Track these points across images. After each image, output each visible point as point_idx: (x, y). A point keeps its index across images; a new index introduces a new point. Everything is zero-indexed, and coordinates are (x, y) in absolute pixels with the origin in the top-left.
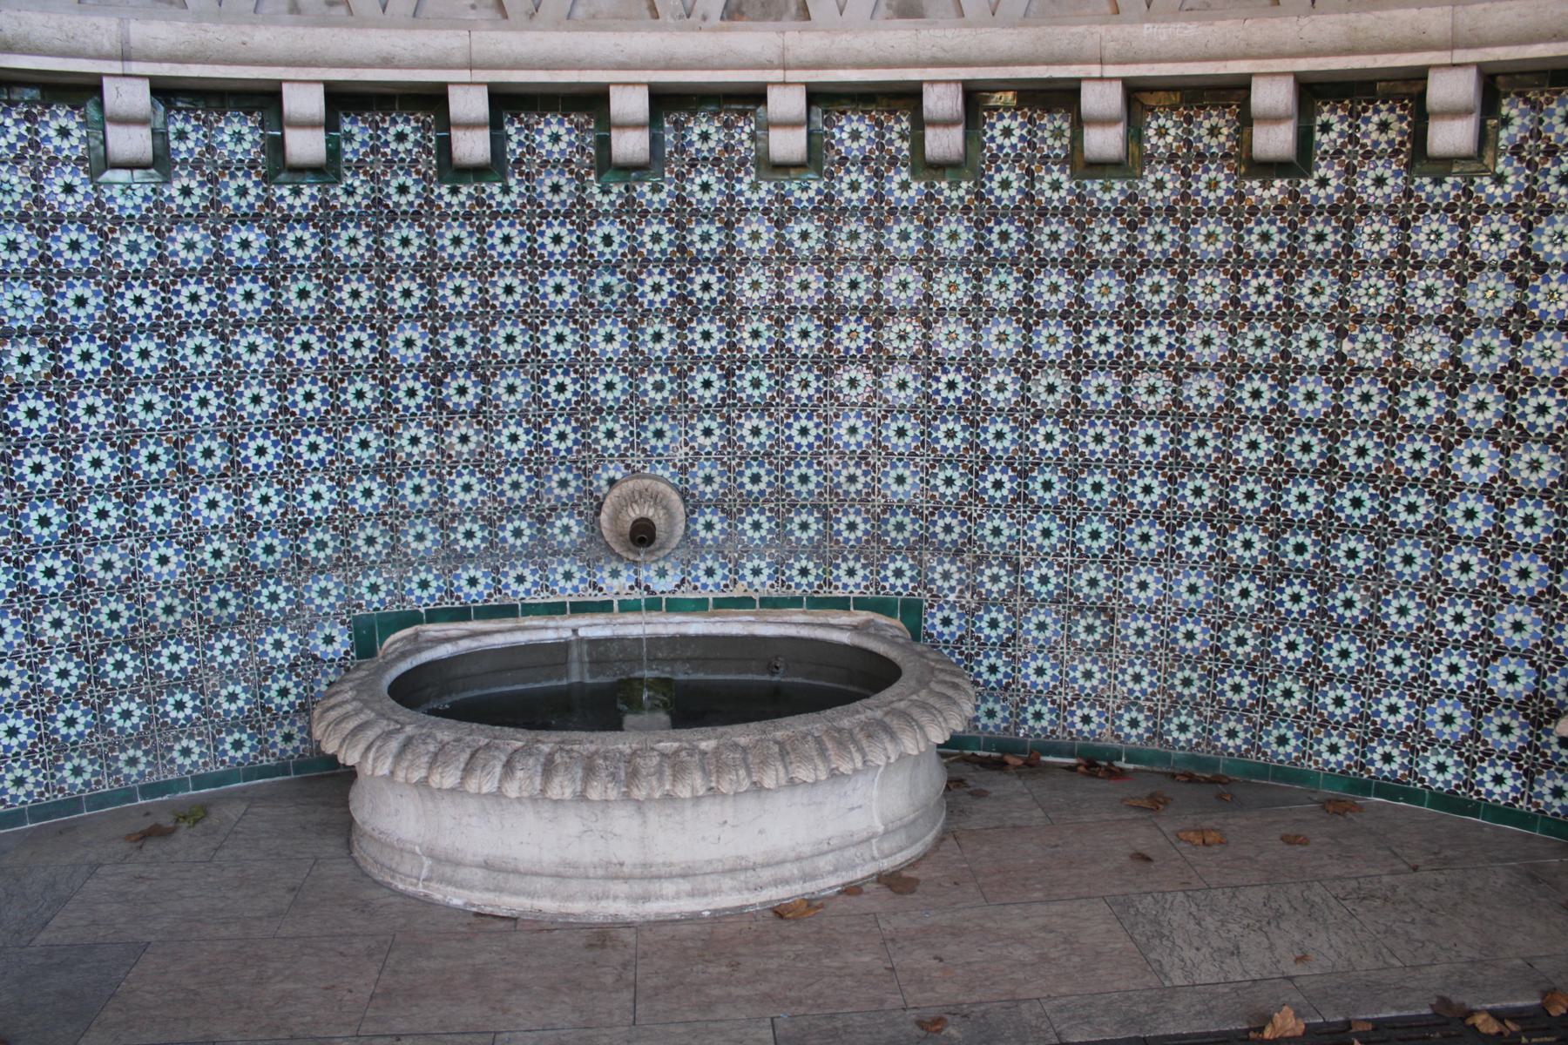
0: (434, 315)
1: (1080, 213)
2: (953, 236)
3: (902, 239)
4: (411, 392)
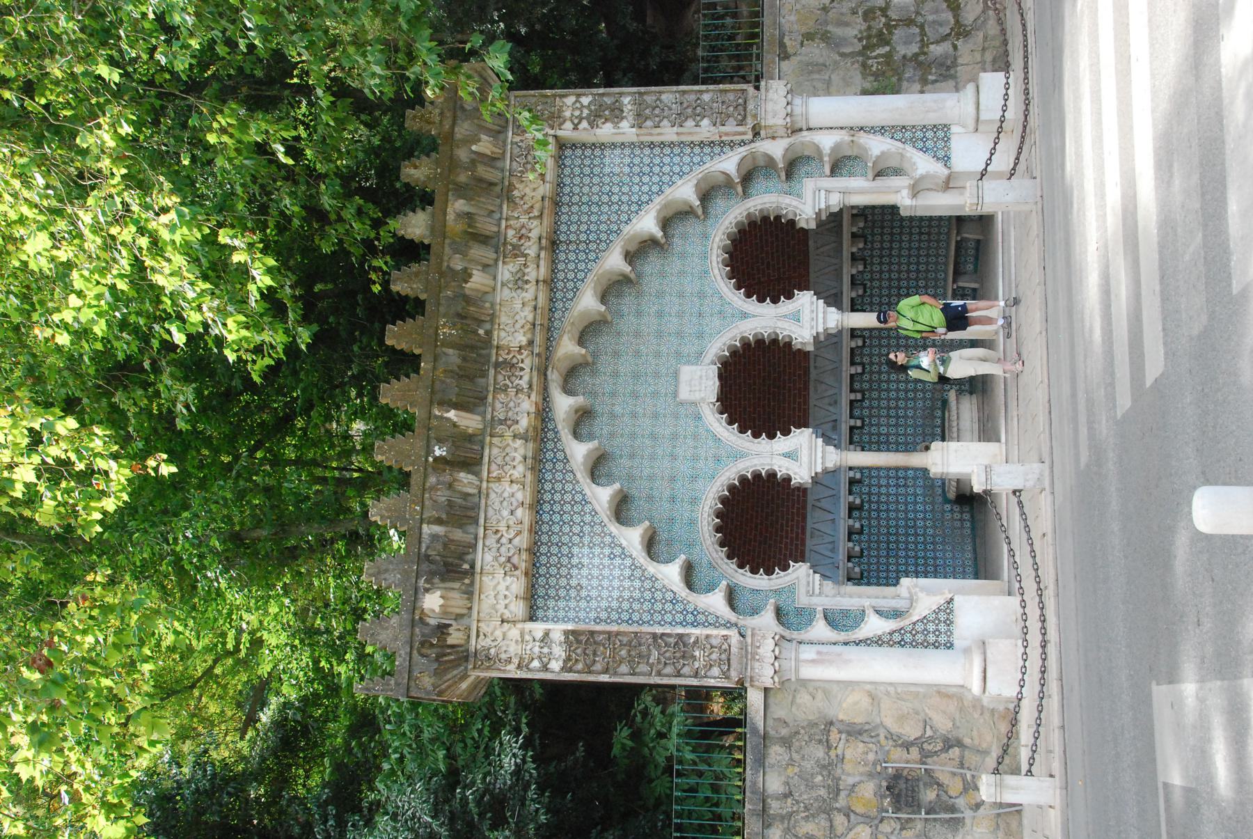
0: (888, 486)
1: (871, 373)
2: (875, 394)
3: (875, 403)
4: (902, 490)
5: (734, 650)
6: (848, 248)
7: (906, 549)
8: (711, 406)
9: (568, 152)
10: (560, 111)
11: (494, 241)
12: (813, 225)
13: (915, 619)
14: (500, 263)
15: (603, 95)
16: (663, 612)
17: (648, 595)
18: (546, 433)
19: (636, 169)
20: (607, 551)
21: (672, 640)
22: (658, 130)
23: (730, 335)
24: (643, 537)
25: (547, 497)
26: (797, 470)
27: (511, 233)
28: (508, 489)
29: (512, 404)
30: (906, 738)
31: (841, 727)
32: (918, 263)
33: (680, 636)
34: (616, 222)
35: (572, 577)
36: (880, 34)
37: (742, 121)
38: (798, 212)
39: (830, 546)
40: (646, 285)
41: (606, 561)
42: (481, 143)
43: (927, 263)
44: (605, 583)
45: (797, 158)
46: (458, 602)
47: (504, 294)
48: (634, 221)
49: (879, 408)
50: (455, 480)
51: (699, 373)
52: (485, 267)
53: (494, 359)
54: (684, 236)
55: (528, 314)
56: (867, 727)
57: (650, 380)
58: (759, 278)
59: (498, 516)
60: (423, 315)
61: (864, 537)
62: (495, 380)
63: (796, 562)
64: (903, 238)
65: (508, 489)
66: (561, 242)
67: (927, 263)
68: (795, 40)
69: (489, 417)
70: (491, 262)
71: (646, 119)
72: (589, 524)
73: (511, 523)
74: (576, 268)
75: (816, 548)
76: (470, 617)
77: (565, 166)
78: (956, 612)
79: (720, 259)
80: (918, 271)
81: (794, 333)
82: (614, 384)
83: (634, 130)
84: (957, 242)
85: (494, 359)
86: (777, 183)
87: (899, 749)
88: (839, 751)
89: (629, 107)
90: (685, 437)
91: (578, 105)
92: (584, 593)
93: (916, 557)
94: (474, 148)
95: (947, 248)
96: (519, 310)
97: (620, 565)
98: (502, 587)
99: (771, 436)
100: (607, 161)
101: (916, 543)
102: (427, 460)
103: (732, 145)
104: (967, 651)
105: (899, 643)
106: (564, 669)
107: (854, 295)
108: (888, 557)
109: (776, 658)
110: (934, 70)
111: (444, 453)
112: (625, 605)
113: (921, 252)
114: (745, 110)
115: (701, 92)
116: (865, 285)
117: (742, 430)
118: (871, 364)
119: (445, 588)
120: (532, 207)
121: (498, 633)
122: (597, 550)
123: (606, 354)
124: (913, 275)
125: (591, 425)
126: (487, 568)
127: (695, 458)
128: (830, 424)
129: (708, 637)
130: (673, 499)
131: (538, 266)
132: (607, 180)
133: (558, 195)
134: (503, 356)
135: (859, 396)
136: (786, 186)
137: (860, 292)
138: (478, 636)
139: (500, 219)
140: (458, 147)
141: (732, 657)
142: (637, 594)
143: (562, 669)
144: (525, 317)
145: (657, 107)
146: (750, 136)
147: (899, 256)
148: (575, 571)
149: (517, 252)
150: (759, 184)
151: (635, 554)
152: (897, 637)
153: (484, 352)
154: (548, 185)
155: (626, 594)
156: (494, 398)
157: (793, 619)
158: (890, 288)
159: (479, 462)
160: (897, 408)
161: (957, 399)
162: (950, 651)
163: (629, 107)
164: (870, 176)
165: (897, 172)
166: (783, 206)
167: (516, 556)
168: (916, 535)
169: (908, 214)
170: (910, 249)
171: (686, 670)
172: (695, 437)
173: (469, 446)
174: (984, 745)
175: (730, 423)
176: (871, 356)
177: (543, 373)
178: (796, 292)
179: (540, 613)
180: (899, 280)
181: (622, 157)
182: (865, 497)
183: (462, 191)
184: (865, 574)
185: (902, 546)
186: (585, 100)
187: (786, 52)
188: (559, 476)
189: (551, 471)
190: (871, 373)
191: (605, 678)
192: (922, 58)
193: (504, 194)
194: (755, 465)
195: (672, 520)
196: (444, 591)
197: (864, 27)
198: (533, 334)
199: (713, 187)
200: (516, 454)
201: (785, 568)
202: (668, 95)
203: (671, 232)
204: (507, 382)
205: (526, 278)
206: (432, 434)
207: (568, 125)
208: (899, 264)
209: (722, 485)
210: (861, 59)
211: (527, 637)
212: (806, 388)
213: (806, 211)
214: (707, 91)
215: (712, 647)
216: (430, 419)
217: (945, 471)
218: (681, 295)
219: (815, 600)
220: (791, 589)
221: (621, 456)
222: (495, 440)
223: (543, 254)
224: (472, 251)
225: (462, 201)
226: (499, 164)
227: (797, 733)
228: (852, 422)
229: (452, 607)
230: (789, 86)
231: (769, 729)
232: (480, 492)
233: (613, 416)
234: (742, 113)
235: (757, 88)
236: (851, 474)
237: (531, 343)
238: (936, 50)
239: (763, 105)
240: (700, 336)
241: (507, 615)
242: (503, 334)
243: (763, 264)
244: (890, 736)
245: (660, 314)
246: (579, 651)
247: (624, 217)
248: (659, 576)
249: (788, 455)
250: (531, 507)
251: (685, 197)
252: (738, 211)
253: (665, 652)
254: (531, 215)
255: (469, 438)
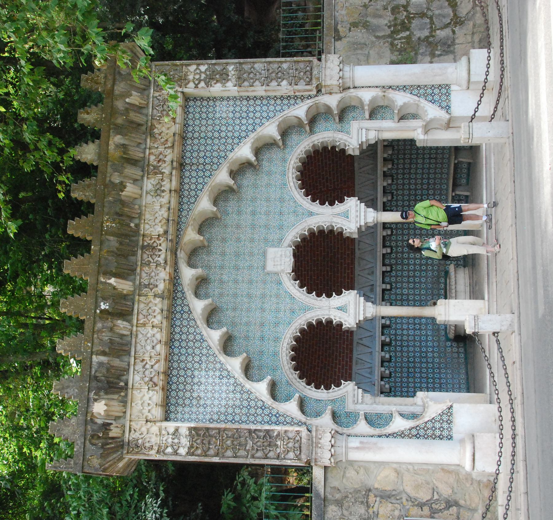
0: (408, 329)
1: (397, 253)
2: (399, 267)
3: (399, 273)
5: (304, 440)
6: (381, 168)
7: (421, 372)
8: (288, 275)
9: (191, 103)
10: (186, 75)
11: (141, 164)
12: (357, 153)
13: (426, 419)
14: (145, 178)
15: (215, 64)
16: (256, 415)
17: (245, 403)
18: (176, 293)
19: (238, 115)
20: (218, 373)
21: (262, 434)
22: (252, 88)
23: (301, 227)
24: (242, 364)
25: (177, 337)
26: (347, 319)
27: (152, 158)
28: (150, 331)
29: (153, 274)
30: (420, 500)
31: (377, 493)
32: (429, 179)
33: (267, 431)
34: (224, 151)
35: (194, 391)
36: (403, 23)
37: (309, 82)
38: (347, 144)
39: (369, 370)
40: (244, 193)
41: (217, 380)
42: (132, 97)
43: (435, 179)
44: (217, 395)
45: (346, 107)
46: (116, 408)
47: (148, 199)
48: (236, 150)
49: (402, 276)
50: (114, 325)
51: (280, 253)
52: (135, 181)
53: (141, 243)
54: (270, 160)
55: (164, 213)
56: (394, 493)
57: (247, 258)
58: (321, 189)
59: (144, 350)
60: (93, 214)
61: (392, 364)
62: (141, 257)
63: (346, 381)
64: (419, 161)
65: (150, 331)
66: (186, 164)
67: (435, 179)
68: (345, 27)
69: (137, 282)
70: (139, 178)
71: (244, 80)
72: (206, 355)
73: (153, 354)
74: (197, 182)
75: (360, 372)
76: (125, 418)
77: (189, 113)
78: (454, 415)
79: (294, 176)
80: (428, 184)
81: (344, 226)
82: (223, 260)
83: (236, 88)
84: (455, 164)
85: (141, 243)
86: (333, 124)
87: (416, 508)
88: (375, 509)
89: (233, 73)
90: (271, 296)
91: (198, 71)
92: (202, 402)
93: (427, 378)
94: (127, 100)
95: (448, 168)
96: (158, 210)
97: (227, 383)
98: (146, 398)
99: (329, 296)
100: (218, 109)
101: (427, 368)
102: (95, 312)
103: (302, 98)
104: (462, 441)
105: (416, 436)
106: (188, 453)
107: (385, 200)
108: (408, 377)
109: (332, 446)
110: (439, 48)
111: (107, 307)
112: (230, 410)
113: (431, 171)
114: (311, 74)
115: (281, 62)
116: (392, 194)
117: (309, 292)
118: (397, 246)
119: (108, 399)
120: (167, 140)
121: (144, 429)
122: (211, 373)
123: (217, 240)
124: (425, 187)
125: (207, 288)
126: (136, 385)
127: (278, 310)
128: (369, 288)
129: (286, 432)
130: (262, 338)
131: (171, 181)
132: (217, 122)
133: (184, 132)
134: (148, 241)
135: (388, 269)
136: (339, 126)
137: (390, 198)
138: (130, 431)
139: (145, 148)
140: (117, 100)
141: (302, 445)
142: (238, 403)
143: (187, 453)
144: (162, 215)
145: (252, 72)
146: (314, 92)
147: (416, 174)
148: (196, 387)
149: (157, 171)
150: (321, 125)
151: (236, 376)
152: (414, 432)
153: (134, 239)
154: (177, 125)
155: (231, 403)
156: (141, 269)
157: (344, 420)
158: (409, 195)
159: (131, 313)
160: (414, 276)
161: (455, 271)
162: (451, 441)
163: (233, 73)
164: (396, 119)
165: (415, 116)
166: (337, 140)
167: (156, 377)
168: (427, 362)
169: (422, 145)
170: (423, 169)
171: (271, 454)
172: (278, 296)
173: (124, 302)
174: (474, 505)
175: (301, 286)
176: (397, 241)
177: (174, 253)
178: (346, 198)
179: (172, 416)
180: (416, 190)
181: (228, 106)
182: (393, 337)
183: (119, 130)
184: (393, 389)
185: (418, 370)
186: (203, 68)
187: (339, 35)
188: (185, 323)
189: (179, 319)
190: (397, 253)
191: (216, 460)
192: (431, 39)
193: (148, 131)
194: (318, 315)
195: (261, 353)
196: (107, 401)
197: (392, 18)
198: (168, 226)
199: (289, 127)
200: (156, 308)
201: (338, 385)
202: (259, 64)
203: (261, 157)
204: (150, 259)
205: (163, 188)
206: (99, 294)
207: (191, 85)
208: (416, 179)
209: (296, 329)
210: (390, 40)
211: (164, 432)
212: (353, 263)
213: (352, 143)
214: (286, 62)
215: (289, 439)
216: (97, 284)
217: (447, 319)
218: (268, 200)
219: (359, 407)
220: (343, 399)
221: (227, 309)
222: (142, 299)
223: (174, 172)
224: (126, 170)
225: (119, 137)
226: (144, 111)
227: (347, 497)
228: (384, 286)
229: (113, 411)
230: (341, 58)
231: (327, 494)
232: (131, 334)
233: (221, 282)
234: (309, 76)
235: (320, 60)
236: (383, 321)
237: (166, 232)
238: (440, 34)
239: (323, 71)
240: (281, 228)
241: (150, 417)
242: (147, 226)
243: (323, 179)
244: (410, 499)
245: (253, 213)
246: (199, 441)
247: (229, 147)
248: (253, 390)
249: (340, 309)
250: (166, 344)
251: (270, 133)
252: (307, 143)
253: (257, 442)
254: (166, 146)
255: (124, 297)
